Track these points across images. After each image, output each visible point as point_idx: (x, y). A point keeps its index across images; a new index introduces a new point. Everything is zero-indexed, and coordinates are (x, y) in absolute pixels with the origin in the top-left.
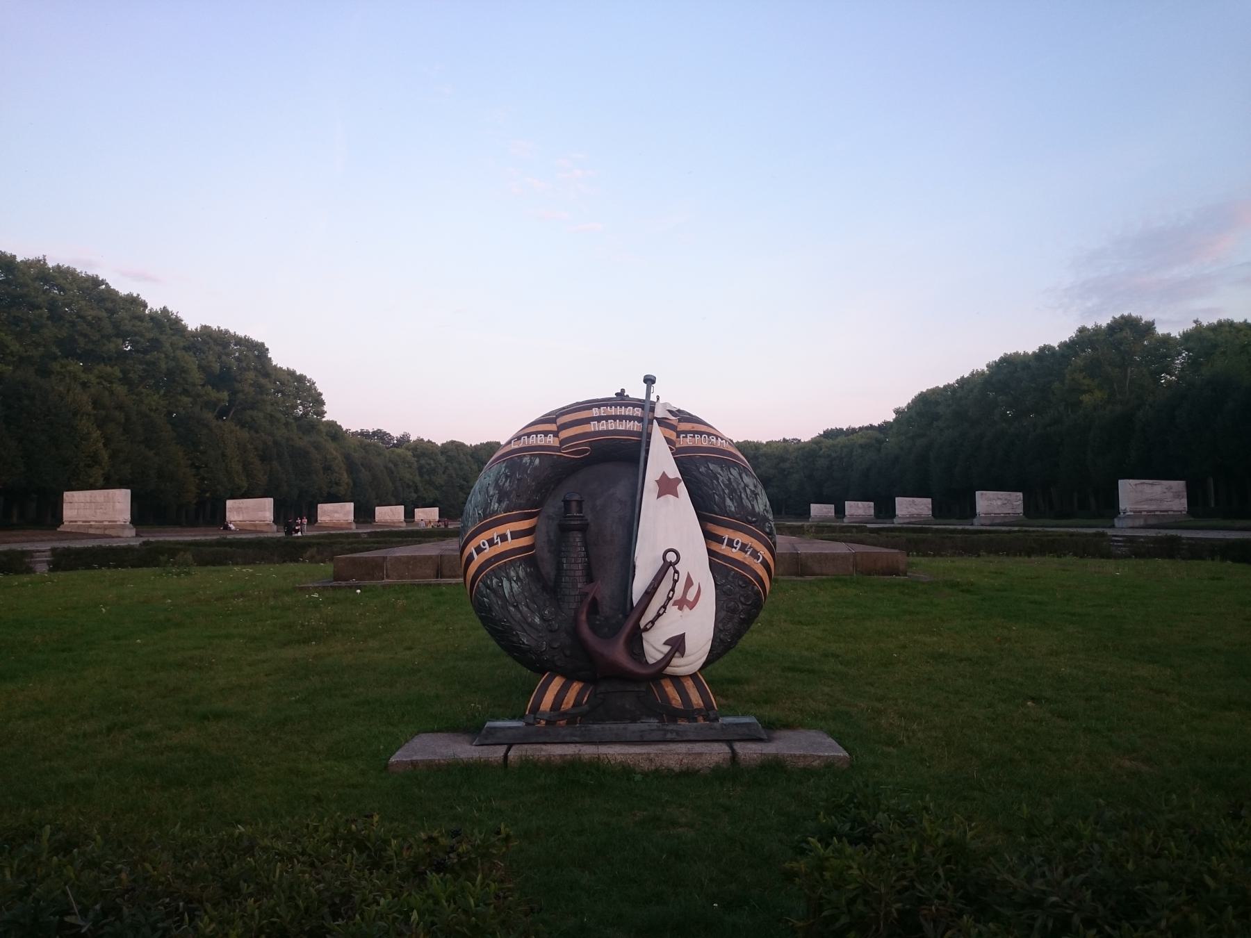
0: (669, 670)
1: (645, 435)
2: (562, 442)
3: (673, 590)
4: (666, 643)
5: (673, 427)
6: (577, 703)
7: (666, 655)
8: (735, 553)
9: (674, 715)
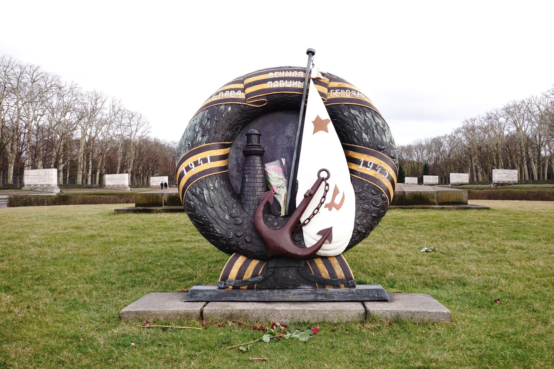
0: (321, 252)
1: (305, 91)
2: (247, 96)
3: (324, 197)
4: (319, 233)
5: (325, 85)
6: (254, 275)
7: (319, 242)
8: (369, 171)
9: (323, 283)
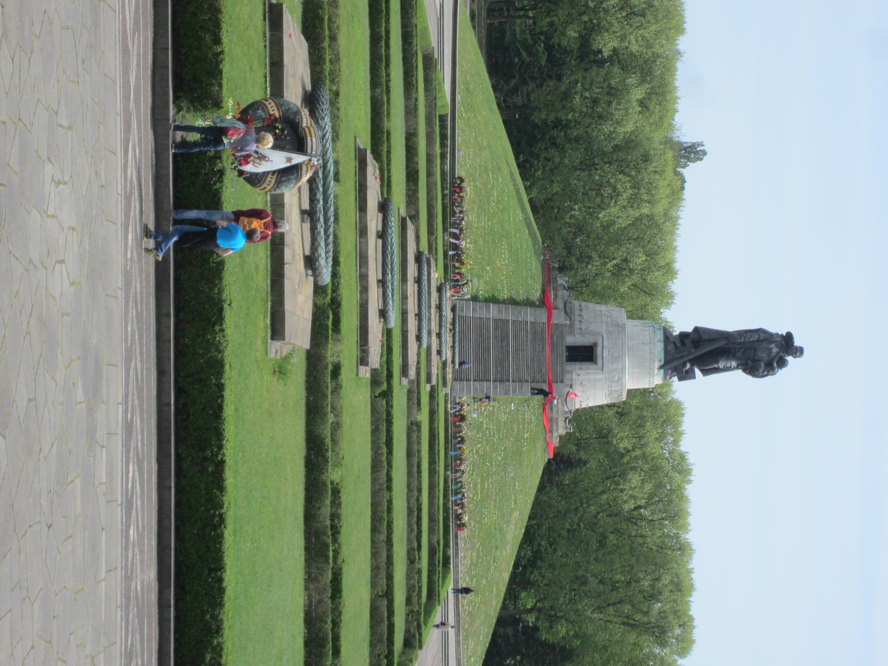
8: (269, 179)
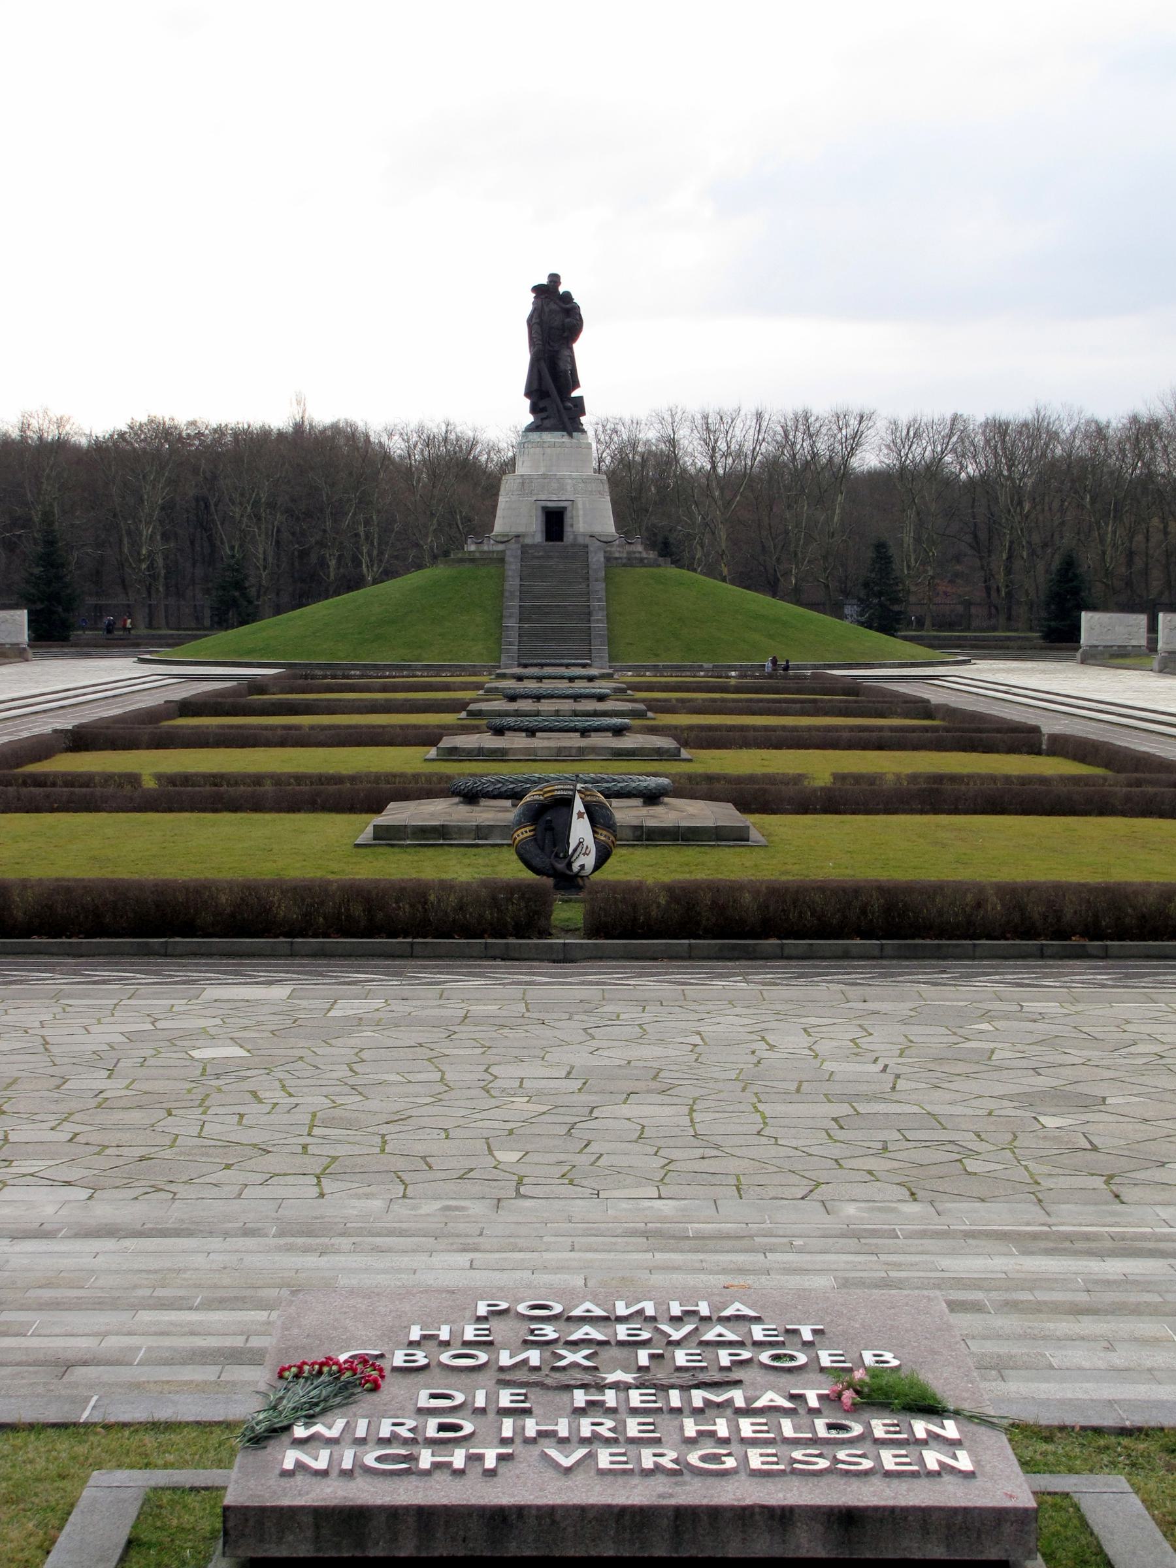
8: (602, 838)
